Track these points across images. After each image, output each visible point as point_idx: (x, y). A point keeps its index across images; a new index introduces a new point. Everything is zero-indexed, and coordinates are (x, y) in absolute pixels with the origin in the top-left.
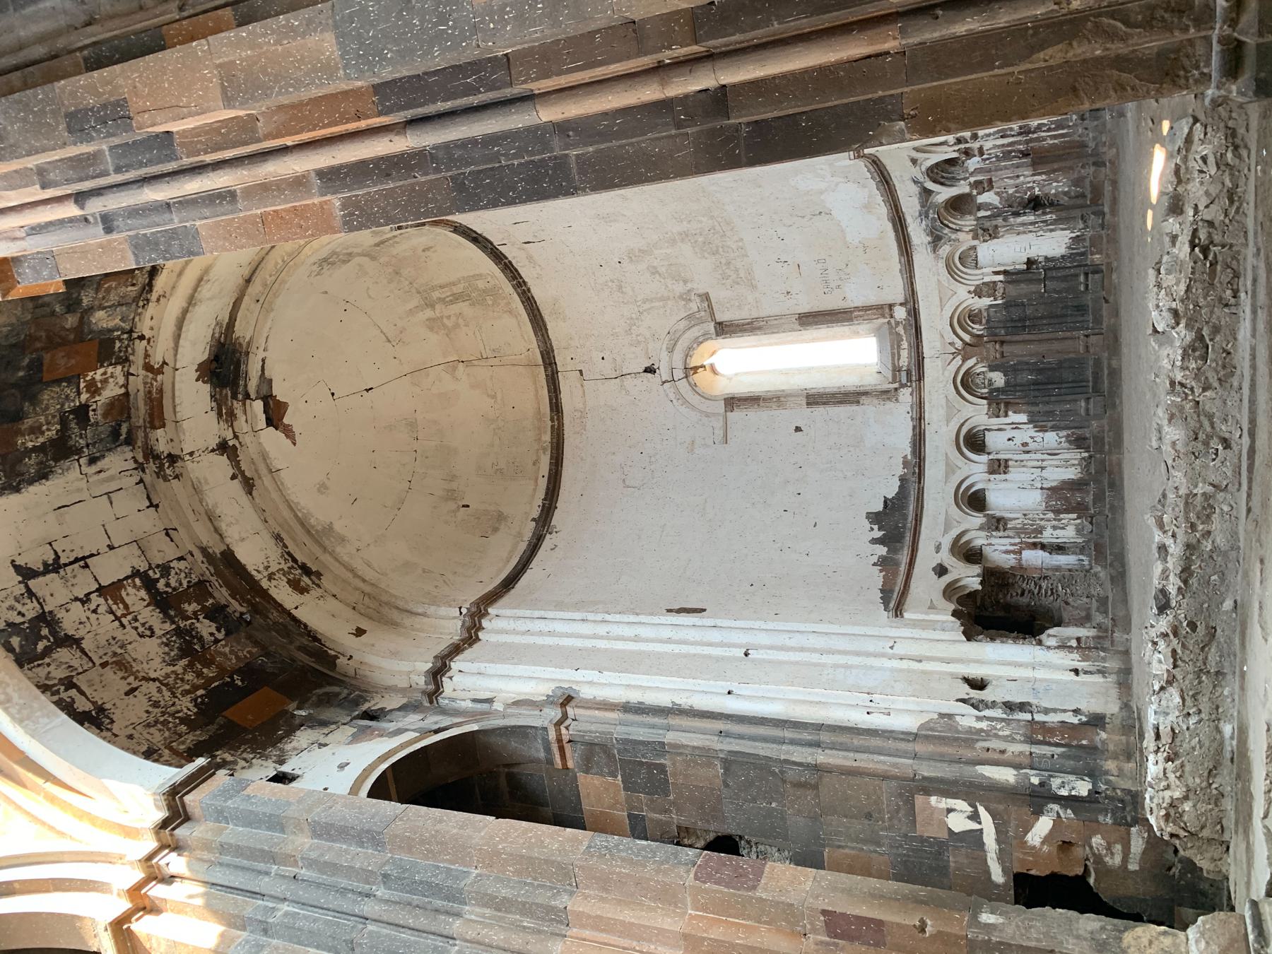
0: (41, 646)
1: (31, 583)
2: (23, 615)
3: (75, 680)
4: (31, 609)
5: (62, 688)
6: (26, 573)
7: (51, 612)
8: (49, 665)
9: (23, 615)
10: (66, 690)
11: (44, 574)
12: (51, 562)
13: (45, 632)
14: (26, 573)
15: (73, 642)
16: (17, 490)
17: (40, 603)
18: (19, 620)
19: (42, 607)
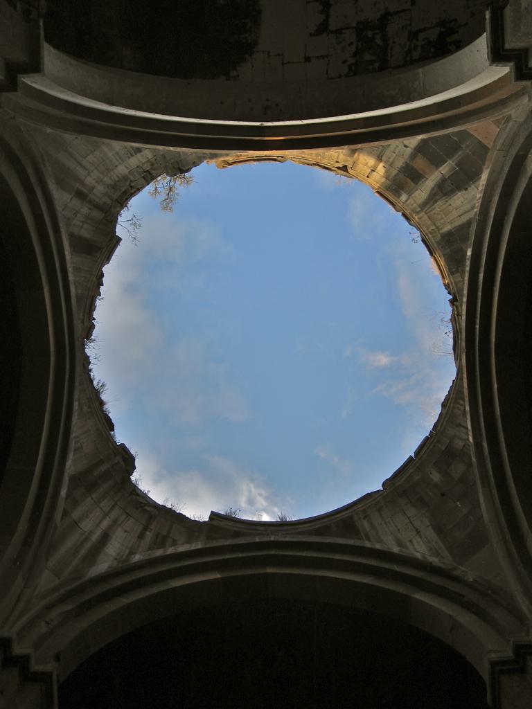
0: (379, 41)
1: (331, 28)
2: (352, 43)
3: (414, 30)
4: (350, 36)
5: (414, 41)
6: (323, 29)
7: (358, 23)
8: (394, 42)
9: (352, 43)
10: (417, 40)
11: (328, 16)
12: (321, 8)
13: (370, 34)
14: (323, 29)
15: (385, 18)
16: (260, 12)
17: (348, 28)
18: (353, 48)
19: (353, 28)
